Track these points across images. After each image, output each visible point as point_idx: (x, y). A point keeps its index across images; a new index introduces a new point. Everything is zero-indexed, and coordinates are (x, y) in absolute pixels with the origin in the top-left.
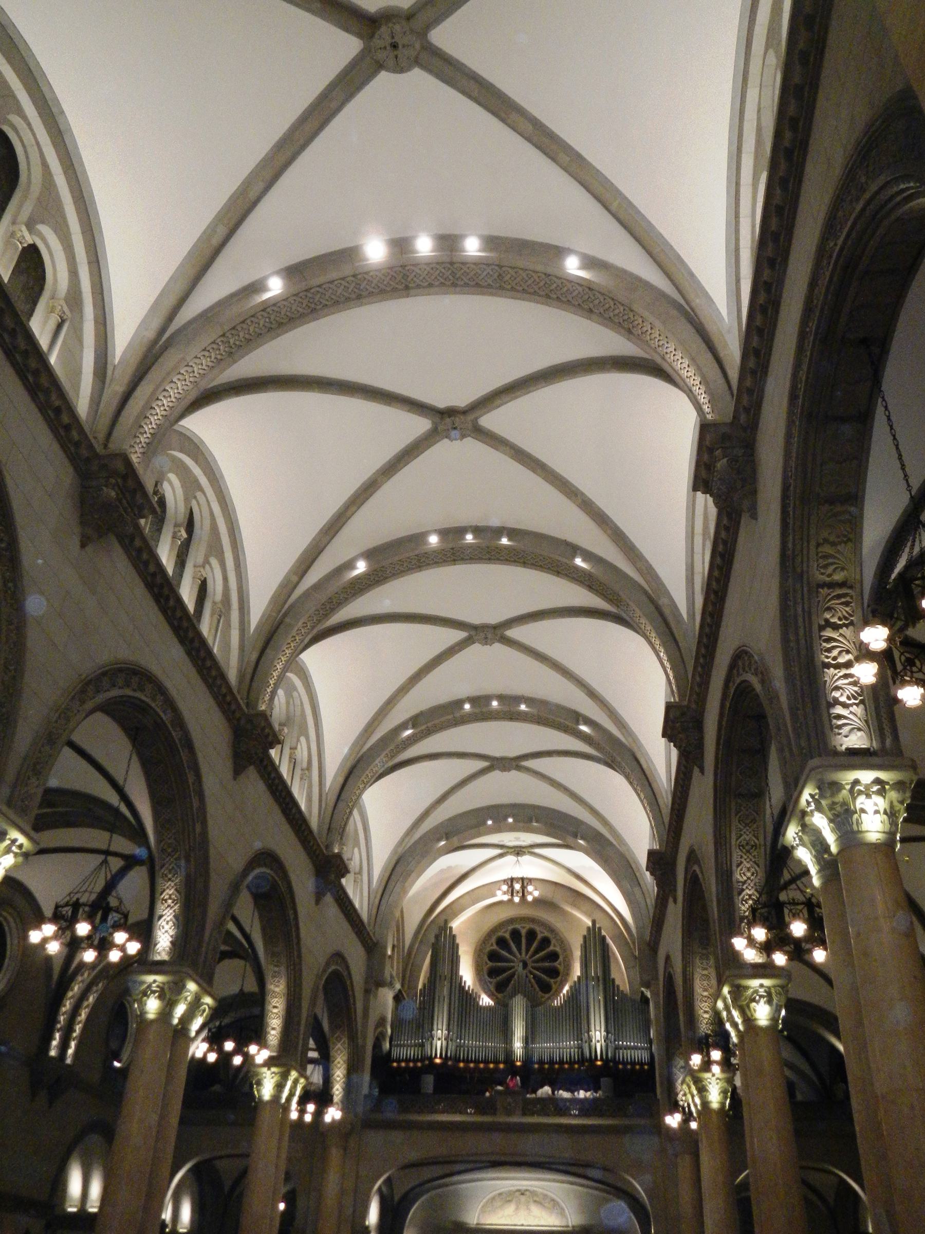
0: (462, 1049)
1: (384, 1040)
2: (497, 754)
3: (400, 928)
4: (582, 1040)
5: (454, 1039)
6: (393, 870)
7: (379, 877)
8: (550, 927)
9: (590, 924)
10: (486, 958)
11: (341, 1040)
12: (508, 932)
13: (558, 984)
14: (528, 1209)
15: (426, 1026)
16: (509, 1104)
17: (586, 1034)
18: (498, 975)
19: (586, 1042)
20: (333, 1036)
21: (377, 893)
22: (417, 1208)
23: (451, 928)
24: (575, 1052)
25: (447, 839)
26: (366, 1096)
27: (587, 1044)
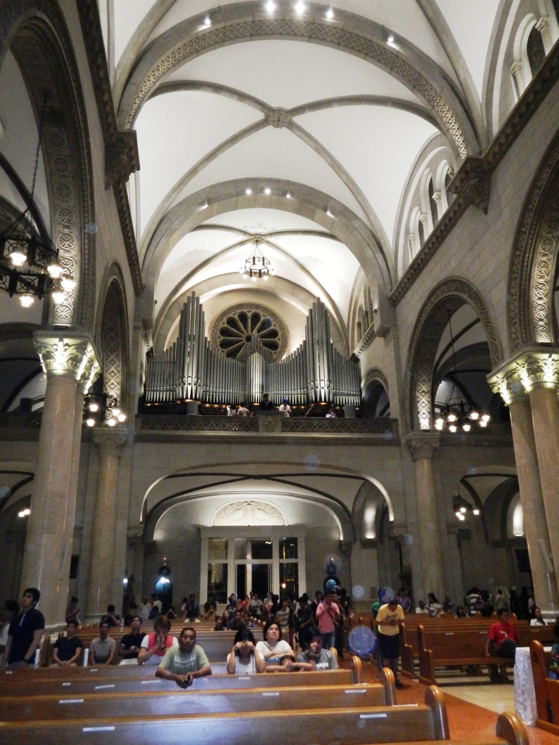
0: (208, 393)
2: (274, 103)
4: (307, 388)
5: (202, 385)
6: (158, 226)
7: (146, 229)
9: (316, 302)
10: (219, 334)
12: (237, 315)
14: (254, 515)
16: (270, 422)
17: (312, 383)
18: (230, 346)
19: (312, 389)
21: (144, 243)
23: (198, 299)
24: (302, 398)
25: (209, 204)
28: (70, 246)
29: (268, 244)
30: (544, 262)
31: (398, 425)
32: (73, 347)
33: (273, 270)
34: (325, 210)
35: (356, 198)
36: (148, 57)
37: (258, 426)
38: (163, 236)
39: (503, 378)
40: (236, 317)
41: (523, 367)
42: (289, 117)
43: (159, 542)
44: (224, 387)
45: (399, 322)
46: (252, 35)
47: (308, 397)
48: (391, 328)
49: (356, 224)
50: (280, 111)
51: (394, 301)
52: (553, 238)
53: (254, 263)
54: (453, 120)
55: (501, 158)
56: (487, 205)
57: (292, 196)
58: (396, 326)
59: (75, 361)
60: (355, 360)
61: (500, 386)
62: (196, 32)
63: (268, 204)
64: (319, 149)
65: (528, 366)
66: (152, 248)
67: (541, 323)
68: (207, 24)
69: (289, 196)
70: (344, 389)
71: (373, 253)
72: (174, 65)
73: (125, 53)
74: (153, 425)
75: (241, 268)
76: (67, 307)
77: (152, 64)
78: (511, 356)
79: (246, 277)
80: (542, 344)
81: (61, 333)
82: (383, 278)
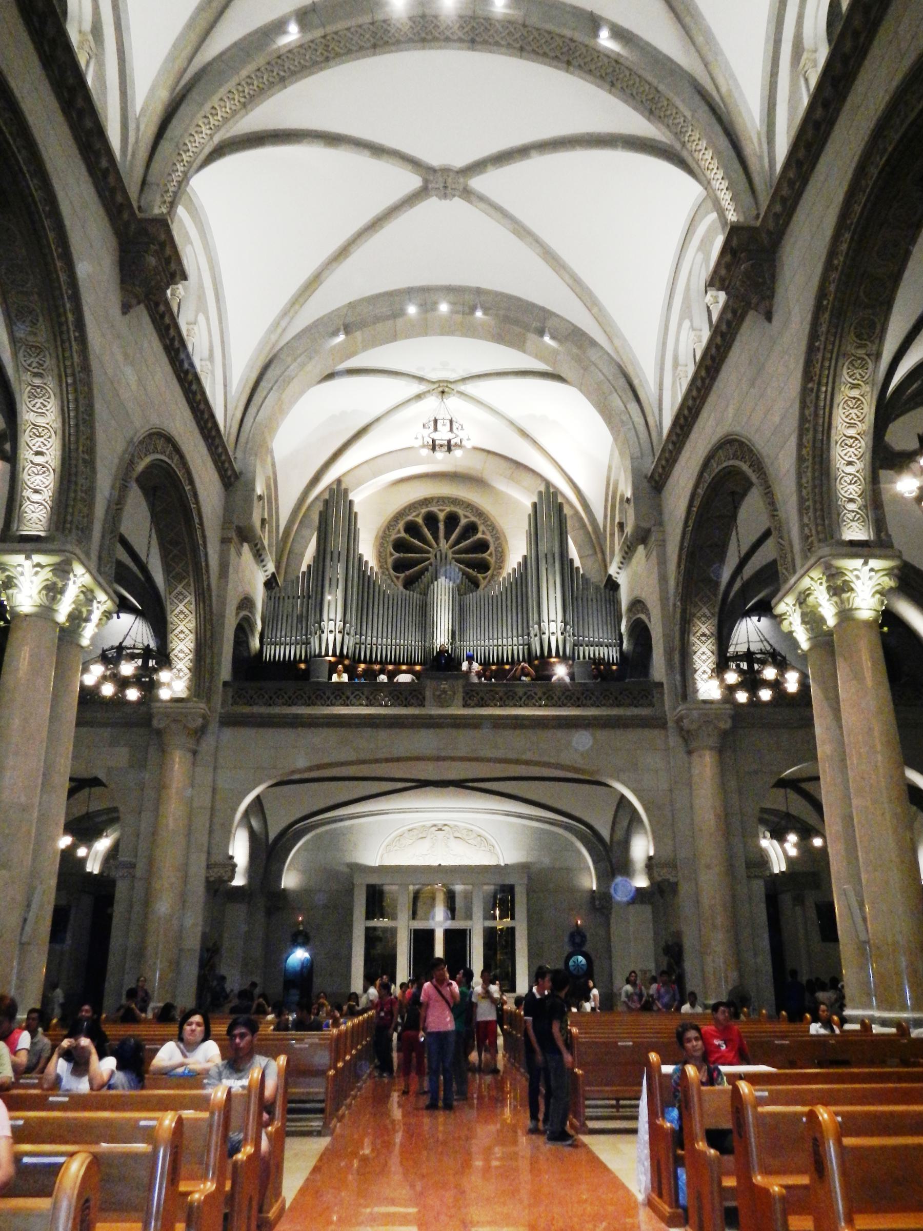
0: (363, 647)
1: (253, 634)
2: (435, 160)
3: (271, 499)
4: (528, 635)
5: (352, 632)
8: (477, 509)
11: (185, 597)
12: (420, 516)
13: (487, 580)
15: (312, 619)
16: (444, 692)
17: (536, 626)
19: (536, 635)
20: (170, 594)
21: (238, 400)
22: (298, 851)
23: (346, 492)
24: (520, 651)
25: (347, 333)
26: (225, 684)
27: (537, 638)
28: (45, 406)
29: (463, 397)
30: (854, 398)
31: (662, 694)
32: (49, 569)
33: (469, 439)
34: (541, 333)
35: (589, 310)
36: (194, 95)
37: (424, 698)
38: (271, 388)
39: (794, 605)
40: (420, 520)
41: (821, 584)
42: (462, 180)
43: (294, 891)
44: (389, 636)
45: (666, 517)
46: (374, 46)
47: (529, 649)
48: (653, 529)
49: (593, 354)
50: (446, 170)
51: (656, 482)
52: (868, 355)
53: (436, 429)
54: (714, 164)
55: (787, 223)
56: (771, 306)
57: (485, 314)
58: (660, 523)
59: (53, 591)
60: (612, 585)
61: (791, 619)
62: (275, 47)
63: (447, 329)
64: (521, 230)
65: (827, 581)
66: (252, 410)
67: (851, 506)
68: (293, 34)
69: (479, 314)
70: (591, 635)
71: (623, 402)
72: (244, 105)
73: (153, 89)
74: (251, 698)
75: (416, 438)
76: (42, 504)
77: (201, 105)
78: (803, 566)
79: (425, 452)
80: (852, 543)
81: (28, 546)
82: (639, 443)
